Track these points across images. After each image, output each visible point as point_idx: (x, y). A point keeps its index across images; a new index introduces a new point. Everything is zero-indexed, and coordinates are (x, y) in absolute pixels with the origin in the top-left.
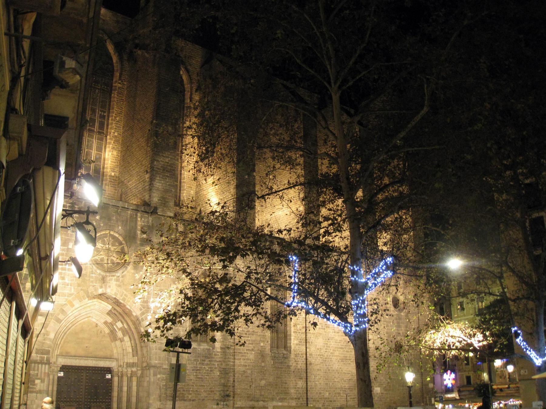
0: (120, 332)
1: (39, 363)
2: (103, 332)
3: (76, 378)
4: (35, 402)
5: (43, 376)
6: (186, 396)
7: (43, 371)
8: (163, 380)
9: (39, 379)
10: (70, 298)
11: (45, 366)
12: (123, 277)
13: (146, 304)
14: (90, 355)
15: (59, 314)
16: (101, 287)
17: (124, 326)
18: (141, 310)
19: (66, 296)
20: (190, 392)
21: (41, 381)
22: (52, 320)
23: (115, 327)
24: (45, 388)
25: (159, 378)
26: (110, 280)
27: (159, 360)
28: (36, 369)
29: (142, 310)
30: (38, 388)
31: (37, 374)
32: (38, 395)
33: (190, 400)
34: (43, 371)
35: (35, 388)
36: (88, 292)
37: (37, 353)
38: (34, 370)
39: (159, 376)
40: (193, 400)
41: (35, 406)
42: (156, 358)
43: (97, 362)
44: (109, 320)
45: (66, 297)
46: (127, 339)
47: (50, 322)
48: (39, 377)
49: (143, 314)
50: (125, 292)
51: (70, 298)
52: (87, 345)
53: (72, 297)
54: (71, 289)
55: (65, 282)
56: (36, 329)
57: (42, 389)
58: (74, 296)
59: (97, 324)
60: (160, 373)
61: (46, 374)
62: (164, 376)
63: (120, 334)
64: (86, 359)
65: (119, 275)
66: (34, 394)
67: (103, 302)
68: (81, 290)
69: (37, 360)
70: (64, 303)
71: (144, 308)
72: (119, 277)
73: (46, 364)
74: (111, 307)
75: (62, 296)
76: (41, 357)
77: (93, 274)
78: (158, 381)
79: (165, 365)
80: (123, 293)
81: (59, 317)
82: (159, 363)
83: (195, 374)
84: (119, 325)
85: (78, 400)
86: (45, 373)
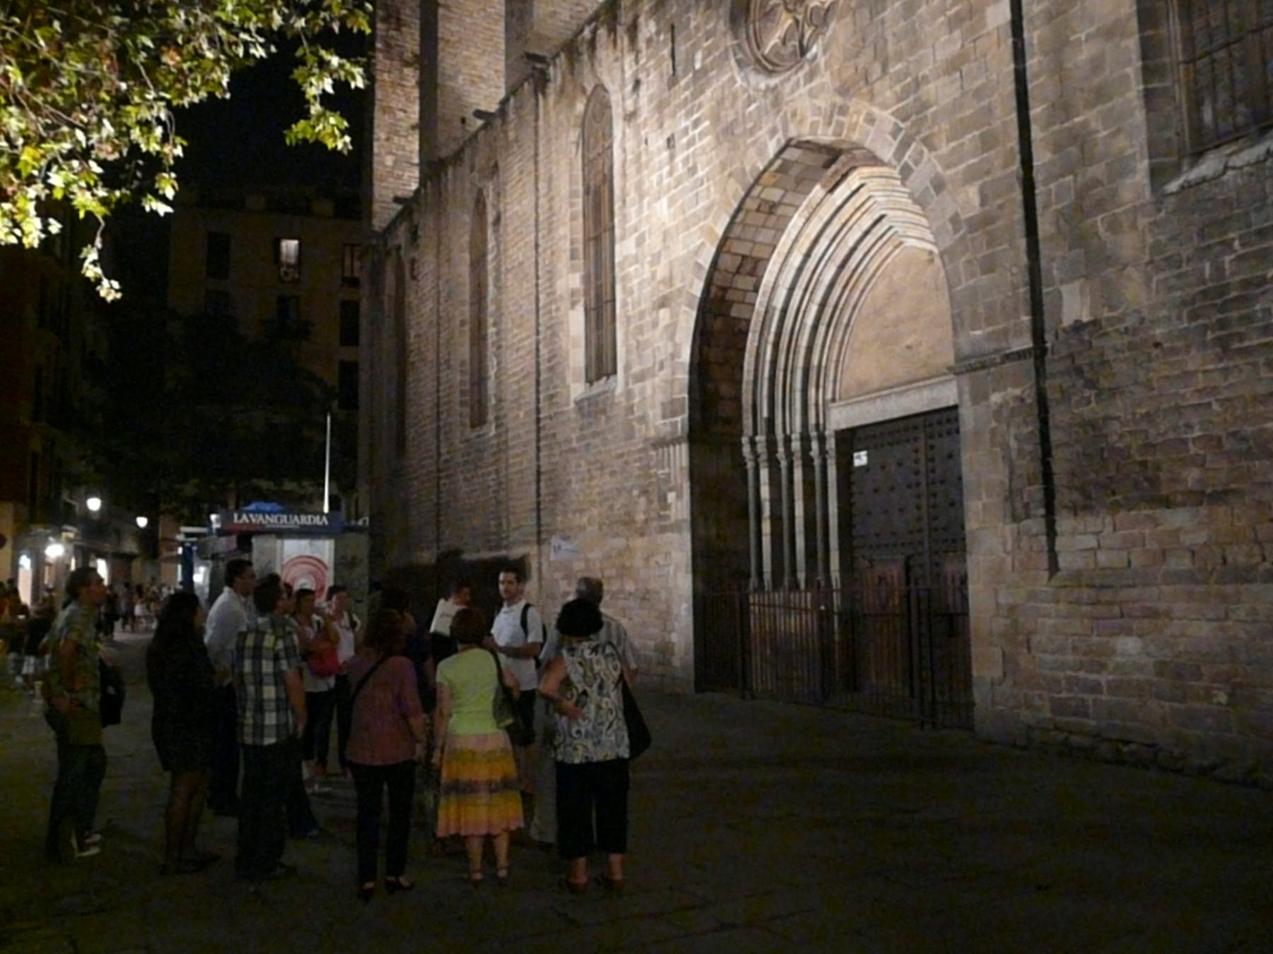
6: (1163, 476)
8: (1013, 413)
10: (709, 220)
12: (825, 52)
13: (911, 99)
14: (923, 372)
15: (691, 285)
16: (773, 132)
19: (700, 220)
20: (1193, 449)
25: (997, 414)
26: (793, 91)
27: (990, 321)
29: (900, 129)
33: (1198, 497)
37: (664, 417)
39: (996, 398)
40: (1219, 497)
41: (672, 569)
42: (975, 314)
43: (935, 393)
45: (702, 224)
48: (672, 484)
52: (909, 341)
54: (708, 188)
58: (716, 208)
64: (901, 393)
68: (730, 175)
70: (698, 243)
71: (904, 120)
72: (815, 57)
78: (994, 424)
79: (1018, 334)
82: (989, 337)
83: (1210, 336)
86: (681, 468)
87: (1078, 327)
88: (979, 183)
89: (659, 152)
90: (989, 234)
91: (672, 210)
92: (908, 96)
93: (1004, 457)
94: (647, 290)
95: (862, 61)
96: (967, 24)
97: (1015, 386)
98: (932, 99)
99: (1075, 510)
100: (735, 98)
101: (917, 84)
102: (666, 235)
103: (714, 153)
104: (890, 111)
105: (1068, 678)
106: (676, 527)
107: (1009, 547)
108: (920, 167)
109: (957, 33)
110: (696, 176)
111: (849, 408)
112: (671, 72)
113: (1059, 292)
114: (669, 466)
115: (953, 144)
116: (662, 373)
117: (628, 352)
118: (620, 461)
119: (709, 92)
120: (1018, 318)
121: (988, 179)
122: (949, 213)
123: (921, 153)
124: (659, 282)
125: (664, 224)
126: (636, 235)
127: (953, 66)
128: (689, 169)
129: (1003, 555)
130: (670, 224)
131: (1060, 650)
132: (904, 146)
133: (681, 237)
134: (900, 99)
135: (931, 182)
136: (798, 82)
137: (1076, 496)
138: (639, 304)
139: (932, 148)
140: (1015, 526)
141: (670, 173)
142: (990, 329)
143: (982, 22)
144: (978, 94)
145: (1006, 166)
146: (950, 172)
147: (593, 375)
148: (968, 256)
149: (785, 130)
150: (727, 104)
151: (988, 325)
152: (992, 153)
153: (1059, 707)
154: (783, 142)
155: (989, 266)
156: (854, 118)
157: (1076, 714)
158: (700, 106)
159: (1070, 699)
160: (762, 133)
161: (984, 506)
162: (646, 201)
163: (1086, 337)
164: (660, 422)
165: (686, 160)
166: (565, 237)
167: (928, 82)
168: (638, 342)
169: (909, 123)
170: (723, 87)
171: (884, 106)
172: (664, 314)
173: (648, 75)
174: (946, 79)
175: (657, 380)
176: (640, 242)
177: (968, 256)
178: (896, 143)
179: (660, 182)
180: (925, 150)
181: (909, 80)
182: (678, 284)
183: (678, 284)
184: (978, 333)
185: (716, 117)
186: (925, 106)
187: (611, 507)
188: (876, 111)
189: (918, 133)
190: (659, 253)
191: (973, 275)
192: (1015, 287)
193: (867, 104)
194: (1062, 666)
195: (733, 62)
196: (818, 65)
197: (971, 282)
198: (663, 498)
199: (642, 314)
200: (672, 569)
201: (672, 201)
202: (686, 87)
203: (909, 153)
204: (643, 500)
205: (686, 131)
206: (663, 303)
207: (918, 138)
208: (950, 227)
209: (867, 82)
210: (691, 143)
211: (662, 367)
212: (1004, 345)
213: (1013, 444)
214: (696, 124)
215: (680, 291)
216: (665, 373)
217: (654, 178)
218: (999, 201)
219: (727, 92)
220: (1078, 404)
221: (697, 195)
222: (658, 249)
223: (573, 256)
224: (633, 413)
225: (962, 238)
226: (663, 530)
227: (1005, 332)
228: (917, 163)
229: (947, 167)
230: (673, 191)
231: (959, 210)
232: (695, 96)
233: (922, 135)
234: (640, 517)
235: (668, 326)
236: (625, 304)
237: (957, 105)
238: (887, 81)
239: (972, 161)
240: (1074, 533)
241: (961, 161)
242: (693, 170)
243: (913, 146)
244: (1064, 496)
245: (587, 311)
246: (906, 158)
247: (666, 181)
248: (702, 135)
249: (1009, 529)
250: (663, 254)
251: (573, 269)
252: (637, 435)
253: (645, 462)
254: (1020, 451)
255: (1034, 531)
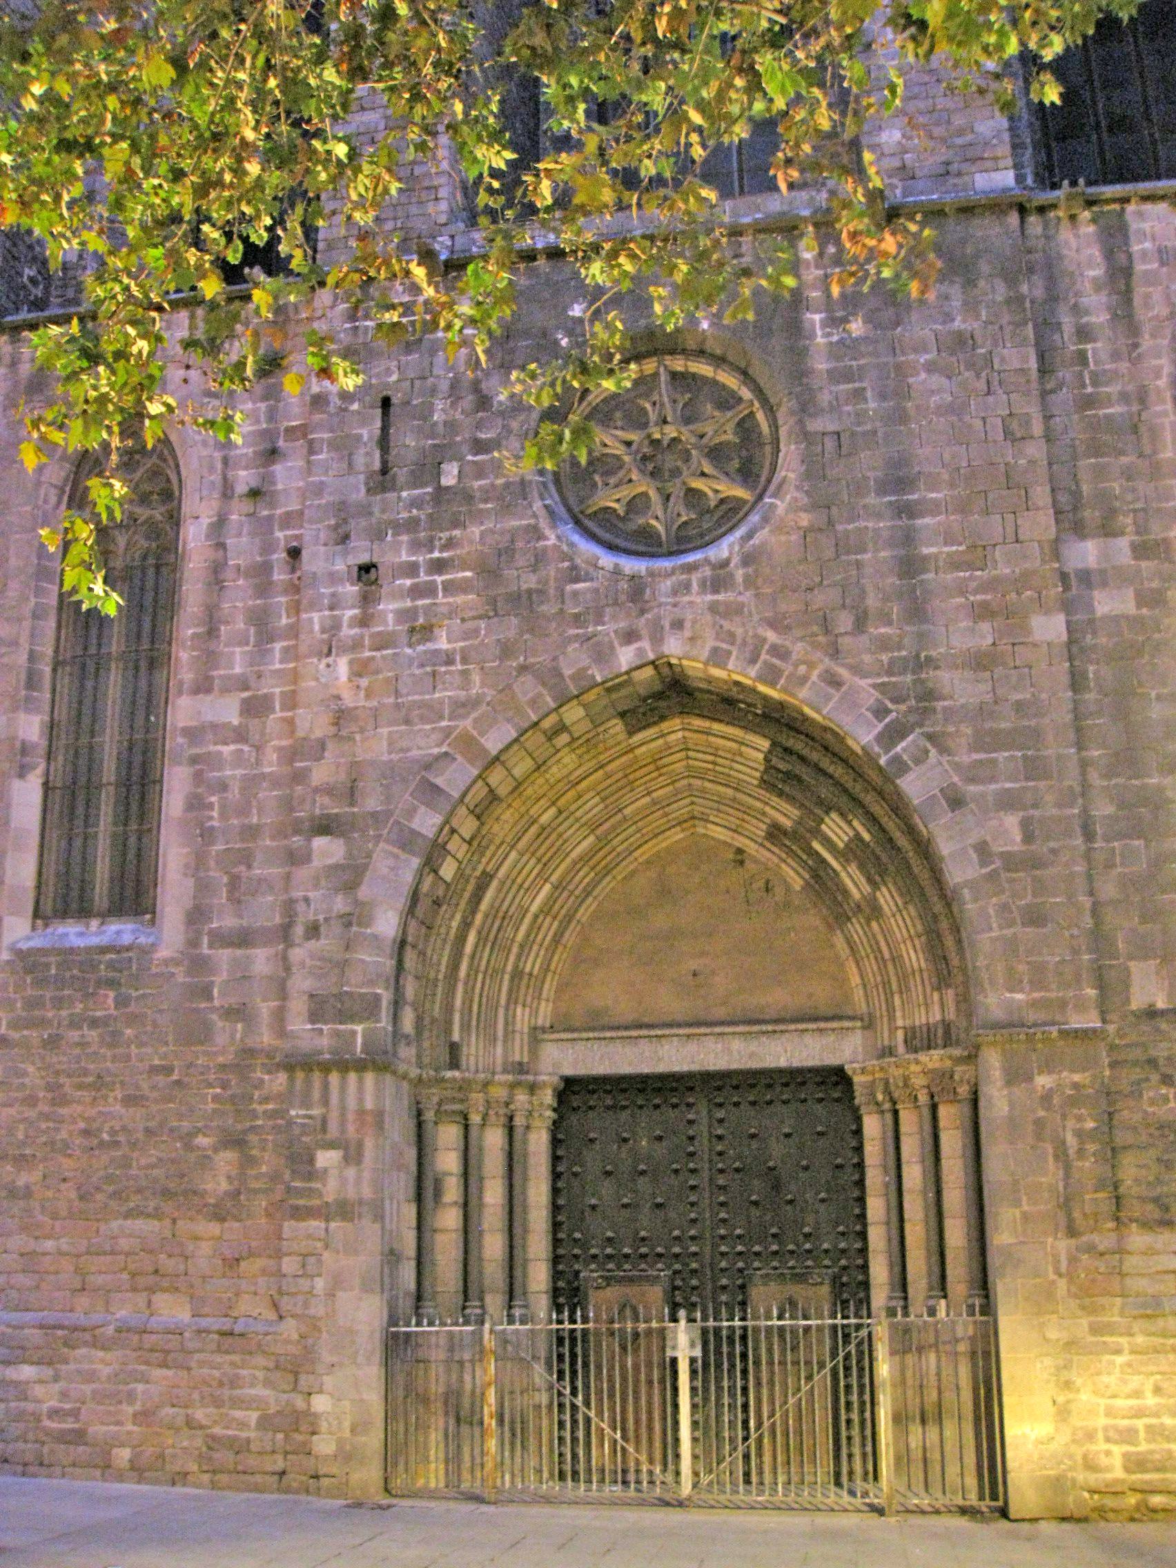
0: (853, 868)
1: (326, 1068)
2: (779, 891)
3: (660, 1138)
4: (320, 1261)
5: (351, 1129)
7: (352, 1104)
8: (1072, 1102)
9: (331, 1145)
10: (467, 724)
11: (361, 1081)
12: (747, 560)
13: (909, 678)
15: (411, 813)
16: (630, 637)
17: (857, 834)
18: (881, 712)
19: (441, 718)
21: (346, 1159)
22: (382, 845)
23: (816, 845)
24: (367, 1192)
25: (1046, 1098)
27: (1038, 983)
28: (316, 1094)
29: (888, 711)
30: (330, 1190)
31: (324, 1121)
32: (333, 1225)
34: (352, 1104)
35: (321, 1195)
36: (561, 675)
37: (314, 1017)
38: (307, 1103)
39: (1043, 1081)
41: (320, 1283)
42: (1010, 970)
43: (753, 1046)
44: (785, 814)
45: (444, 723)
46: (886, 898)
47: (369, 856)
48: (333, 1131)
49: (893, 734)
50: (771, 636)
51: (467, 724)
52: (693, 965)
53: (474, 715)
54: (465, 673)
55: (436, 652)
56: (307, 900)
57: (351, 1193)
58: (483, 708)
59: (740, 851)
60: (1048, 1067)
61: (369, 1119)
62: (1077, 1077)
63: (853, 880)
65: (725, 554)
66: (315, 1225)
67: (717, 727)
68: (523, 669)
69: (320, 1053)
70: (436, 751)
71: (895, 701)
72: (725, 564)
73: (361, 1066)
74: (765, 744)
75: (423, 719)
76: (337, 1034)
77: (577, 580)
78: (1041, 1113)
79: (1081, 1007)
80: (764, 640)
81: (415, 824)
82: (1034, 1004)
84: (837, 829)
85: (677, 1250)
86: (361, 1113)
87: (1152, 1013)
88: (1021, 814)
89: (333, 578)
90: (1034, 878)
91: (364, 682)
92: (903, 672)
93: (1056, 1157)
94: (268, 795)
95: (820, 599)
96: (999, 622)
97: (1073, 1071)
98: (946, 691)
99: (1146, 1225)
100: (539, 559)
101: (920, 664)
102: (341, 717)
103: (483, 624)
104: (870, 681)
105: (1149, 1428)
106: (344, 1210)
107: (1063, 1269)
108: (923, 767)
109: (985, 627)
110: (430, 646)
111: (580, 1046)
112: (377, 465)
113: (1127, 969)
114: (325, 1101)
115: (976, 756)
116: (313, 944)
117: (203, 887)
118: (161, 1080)
119: (475, 531)
120: (1081, 989)
121: (1036, 813)
122: (973, 838)
123: (927, 752)
124: (316, 790)
125: (339, 698)
126: (246, 694)
127: (981, 662)
128: (412, 630)
129: (1052, 1276)
130: (349, 700)
131: (1137, 1394)
132: (893, 734)
133: (384, 731)
134: (890, 673)
135: (942, 790)
136: (687, 586)
137: (1153, 1212)
138: (243, 811)
139: (943, 750)
140: (1073, 1242)
141: (364, 621)
142: (1036, 995)
143: (1027, 631)
144: (1019, 706)
145: (1059, 805)
146: (973, 788)
147: (47, 906)
148: (1004, 898)
149: (657, 638)
150: (521, 561)
151: (1031, 991)
152: (1042, 784)
153: (1136, 1463)
154: (651, 656)
155: (1035, 918)
156: (802, 669)
157: (1158, 1470)
158: (450, 544)
159: (1152, 1452)
160: (608, 628)
161: (1026, 1217)
162: (278, 646)
163: (1164, 1026)
164: (299, 1025)
165: (405, 615)
166: (15, 643)
167: (937, 668)
168: (234, 883)
169: (903, 707)
170: (513, 535)
171: (857, 670)
172: (327, 849)
173: (311, 451)
174: (968, 674)
175: (296, 954)
176: (255, 708)
177: (1004, 898)
178: (880, 726)
179: (334, 627)
180: (933, 752)
181: (904, 653)
182: (372, 803)
183: (372, 803)
184: (1019, 996)
185: (489, 571)
186: (929, 695)
187: (126, 1163)
188: (844, 673)
189: (921, 725)
190: (322, 745)
191: (1011, 924)
192: (1075, 952)
193: (827, 660)
194: (1139, 1413)
195: (537, 505)
196: (731, 575)
197: (1008, 932)
198: (302, 1163)
199: (251, 832)
200: (320, 1283)
201: (360, 670)
202: (416, 503)
203: (904, 744)
204: (226, 1160)
205: (412, 569)
206: (325, 827)
207: (918, 730)
208: (974, 856)
209: (827, 632)
210: (417, 592)
211: (313, 931)
212: (1058, 1018)
213: (1071, 1140)
214: (439, 566)
215: (374, 815)
216: (326, 944)
217: (316, 619)
218: (1052, 844)
219: (520, 544)
220: (1152, 1102)
221: (434, 674)
222: (318, 733)
223: (32, 681)
224: (210, 998)
225: (992, 877)
226: (299, 1214)
227: (1063, 1004)
228: (918, 762)
229: (972, 780)
230: (368, 654)
231: (988, 838)
232: (434, 522)
233: (926, 729)
234: (217, 1184)
235: (337, 867)
236: (195, 804)
237: (982, 712)
238: (864, 638)
239: (1008, 785)
240: (1150, 1252)
241: (993, 779)
242: (426, 632)
243: (911, 738)
244: (1135, 1209)
245: (46, 785)
246: (899, 748)
247: (347, 632)
248: (449, 588)
249: (1063, 1245)
250: (330, 746)
251: (29, 705)
252: (221, 1039)
253: (235, 1089)
254: (1081, 1152)
255: (1101, 1248)
